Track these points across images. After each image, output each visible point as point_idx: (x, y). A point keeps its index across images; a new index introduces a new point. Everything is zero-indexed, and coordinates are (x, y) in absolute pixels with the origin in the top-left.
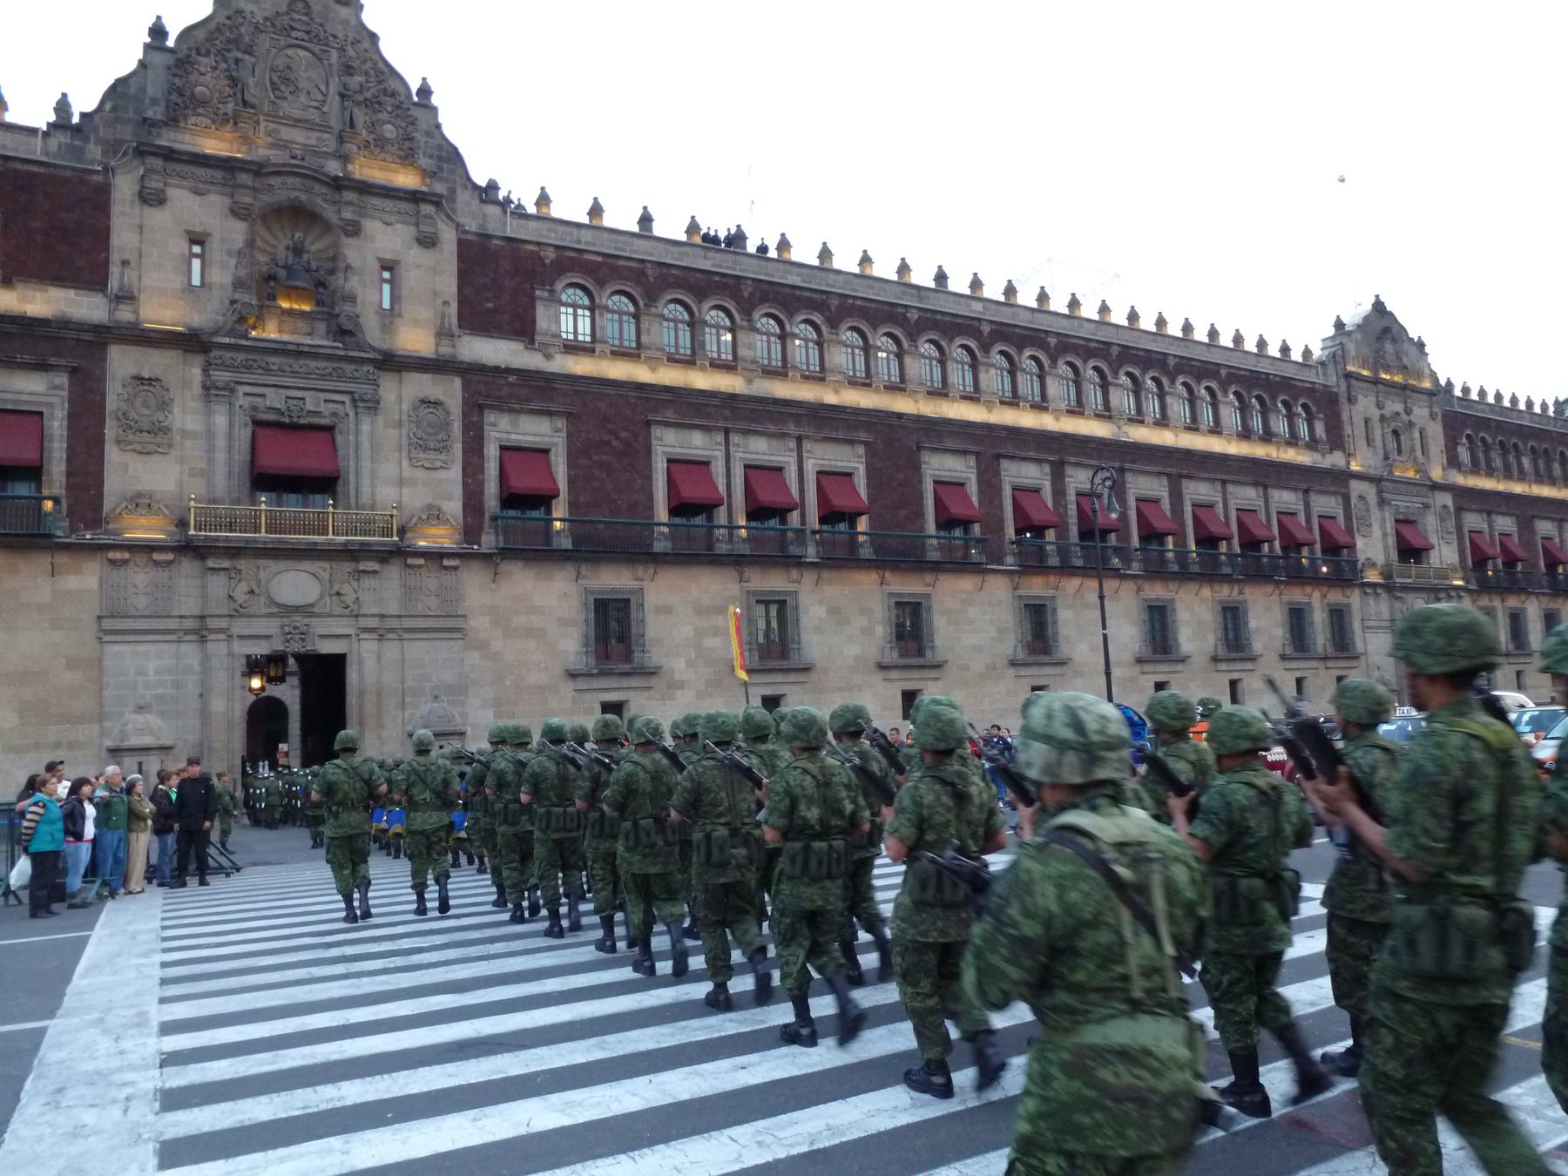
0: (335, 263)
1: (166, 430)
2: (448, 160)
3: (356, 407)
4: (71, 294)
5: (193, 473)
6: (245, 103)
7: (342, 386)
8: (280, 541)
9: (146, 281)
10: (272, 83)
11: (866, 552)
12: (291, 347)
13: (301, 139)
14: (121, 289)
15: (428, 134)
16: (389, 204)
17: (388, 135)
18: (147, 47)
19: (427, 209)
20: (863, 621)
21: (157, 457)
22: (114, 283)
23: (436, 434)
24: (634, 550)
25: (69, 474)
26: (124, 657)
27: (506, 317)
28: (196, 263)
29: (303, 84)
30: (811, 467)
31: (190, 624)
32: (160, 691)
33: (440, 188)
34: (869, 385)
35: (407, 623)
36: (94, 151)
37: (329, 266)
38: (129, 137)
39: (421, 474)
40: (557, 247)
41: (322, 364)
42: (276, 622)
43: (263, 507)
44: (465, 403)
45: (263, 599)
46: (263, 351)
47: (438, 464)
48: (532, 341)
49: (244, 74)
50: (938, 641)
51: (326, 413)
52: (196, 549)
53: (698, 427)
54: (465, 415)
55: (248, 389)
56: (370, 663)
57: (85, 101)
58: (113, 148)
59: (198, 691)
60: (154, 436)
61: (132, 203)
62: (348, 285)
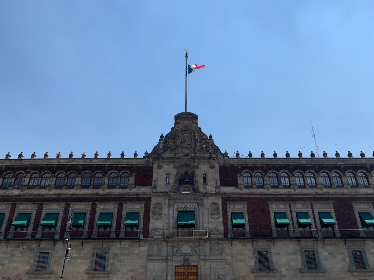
0: (193, 175)
3: (198, 206)
6: (176, 146)
7: (195, 201)
8: (183, 238)
9: (158, 184)
11: (338, 235)
13: (187, 151)
14: (154, 186)
15: (212, 145)
17: (203, 147)
18: (160, 140)
19: (212, 161)
20: (341, 257)
22: (153, 185)
23: (216, 210)
24: (268, 236)
25: (143, 225)
26: (151, 265)
27: (231, 182)
28: (168, 178)
29: (187, 140)
30: (316, 211)
31: (164, 258)
32: (158, 274)
33: (214, 156)
34: (332, 187)
35: (211, 258)
36: (151, 160)
39: (213, 220)
40: (241, 164)
42: (182, 258)
44: (222, 203)
45: (179, 252)
47: (217, 218)
48: (237, 187)
50: (370, 263)
51: (192, 208)
52: (166, 240)
53: (281, 203)
54: (222, 205)
55: (176, 204)
56: (203, 268)
59: (166, 275)
61: (157, 169)
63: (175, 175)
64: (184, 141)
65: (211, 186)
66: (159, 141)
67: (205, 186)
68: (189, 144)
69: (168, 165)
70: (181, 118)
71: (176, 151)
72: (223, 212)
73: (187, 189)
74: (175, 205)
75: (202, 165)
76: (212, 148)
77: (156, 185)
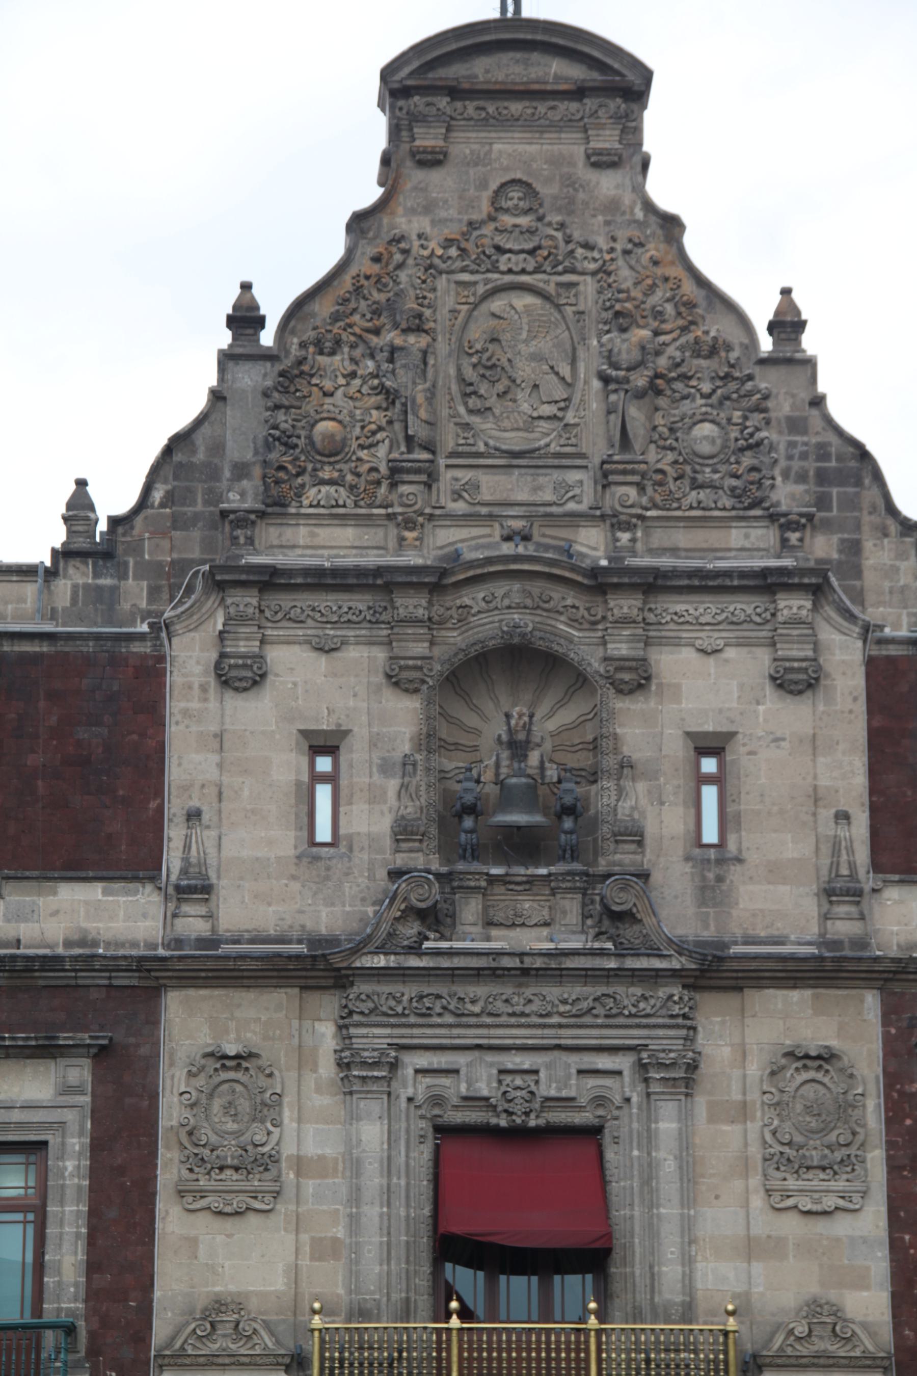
0: (599, 757)
1: (268, 1162)
2: (842, 477)
3: (646, 1080)
4: (94, 892)
5: (324, 1250)
6: (409, 440)
9: (230, 850)
10: (462, 380)
12: (507, 962)
13: (522, 496)
14: (184, 872)
15: (796, 425)
16: (704, 608)
17: (706, 448)
18: (226, 359)
19: (793, 605)
21: (253, 1220)
22: (172, 861)
23: (824, 1130)
25: (92, 1267)
28: (323, 794)
29: (525, 370)
33: (823, 547)
36: (135, 592)
37: (582, 760)
38: (196, 554)
39: (791, 1226)
41: (575, 990)
43: (455, 1322)
46: (453, 974)
47: (830, 1202)
49: (401, 378)
51: (583, 1101)
55: (423, 1060)
57: (115, 497)
58: (170, 580)
60: (248, 1178)
61: (204, 689)
62: (624, 807)
63: (398, 756)
64: (490, 369)
65: (776, 872)
66: (212, 380)
67: (711, 875)
68: (547, 410)
69: (324, 649)
70: (455, 92)
71: (404, 489)
72: (890, 1145)
73: (526, 904)
74: (410, 1071)
75: (688, 653)
76: (796, 465)
77: (203, 863)
